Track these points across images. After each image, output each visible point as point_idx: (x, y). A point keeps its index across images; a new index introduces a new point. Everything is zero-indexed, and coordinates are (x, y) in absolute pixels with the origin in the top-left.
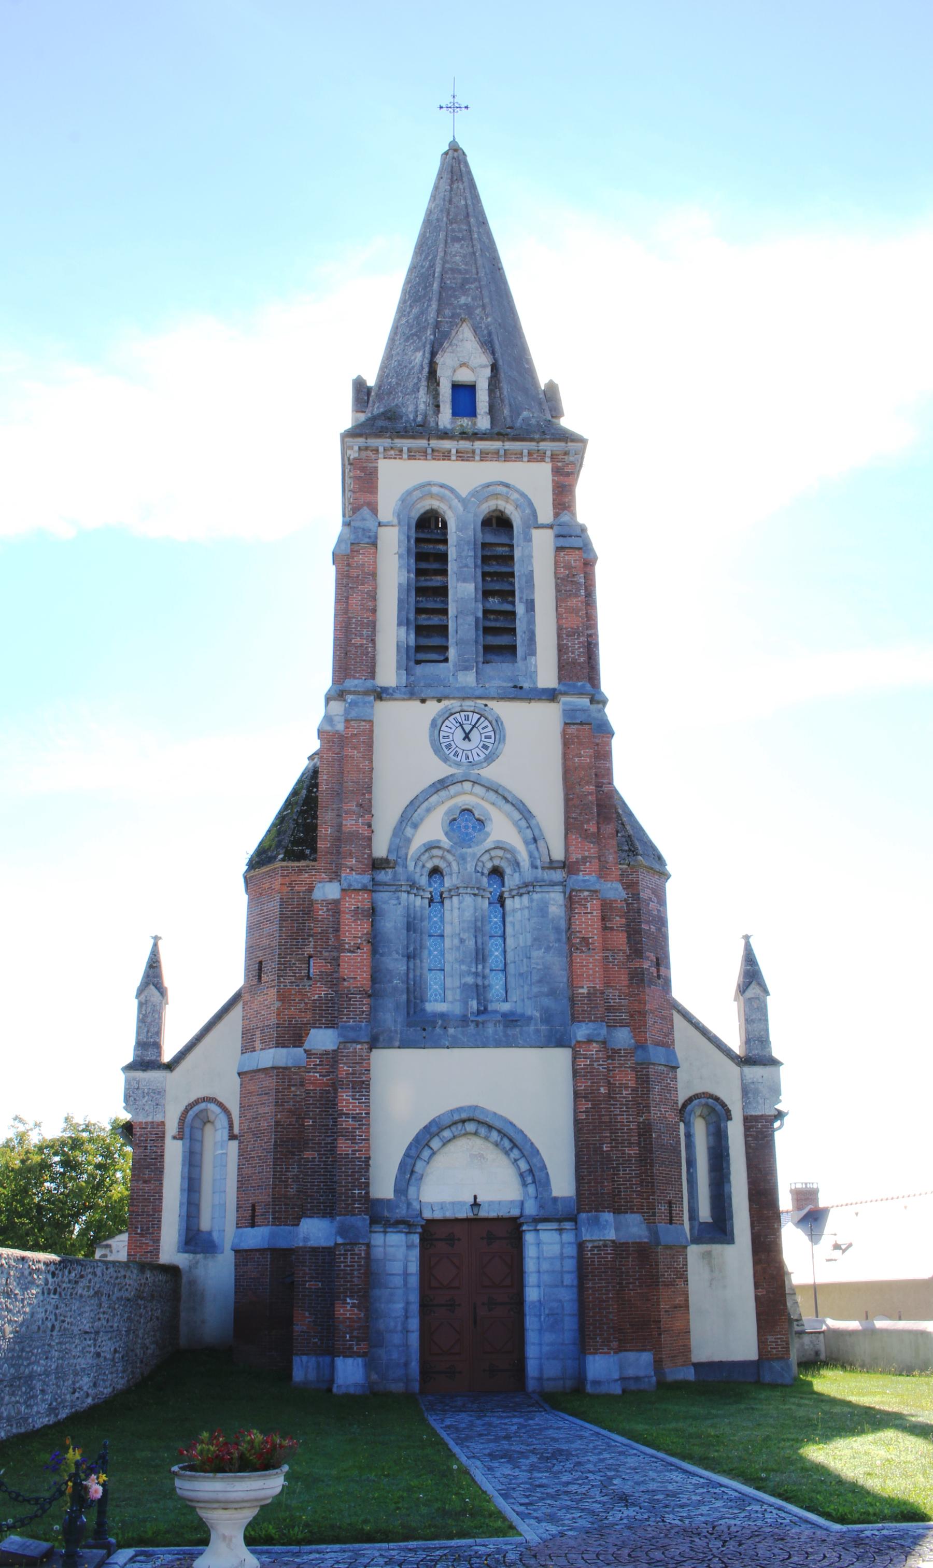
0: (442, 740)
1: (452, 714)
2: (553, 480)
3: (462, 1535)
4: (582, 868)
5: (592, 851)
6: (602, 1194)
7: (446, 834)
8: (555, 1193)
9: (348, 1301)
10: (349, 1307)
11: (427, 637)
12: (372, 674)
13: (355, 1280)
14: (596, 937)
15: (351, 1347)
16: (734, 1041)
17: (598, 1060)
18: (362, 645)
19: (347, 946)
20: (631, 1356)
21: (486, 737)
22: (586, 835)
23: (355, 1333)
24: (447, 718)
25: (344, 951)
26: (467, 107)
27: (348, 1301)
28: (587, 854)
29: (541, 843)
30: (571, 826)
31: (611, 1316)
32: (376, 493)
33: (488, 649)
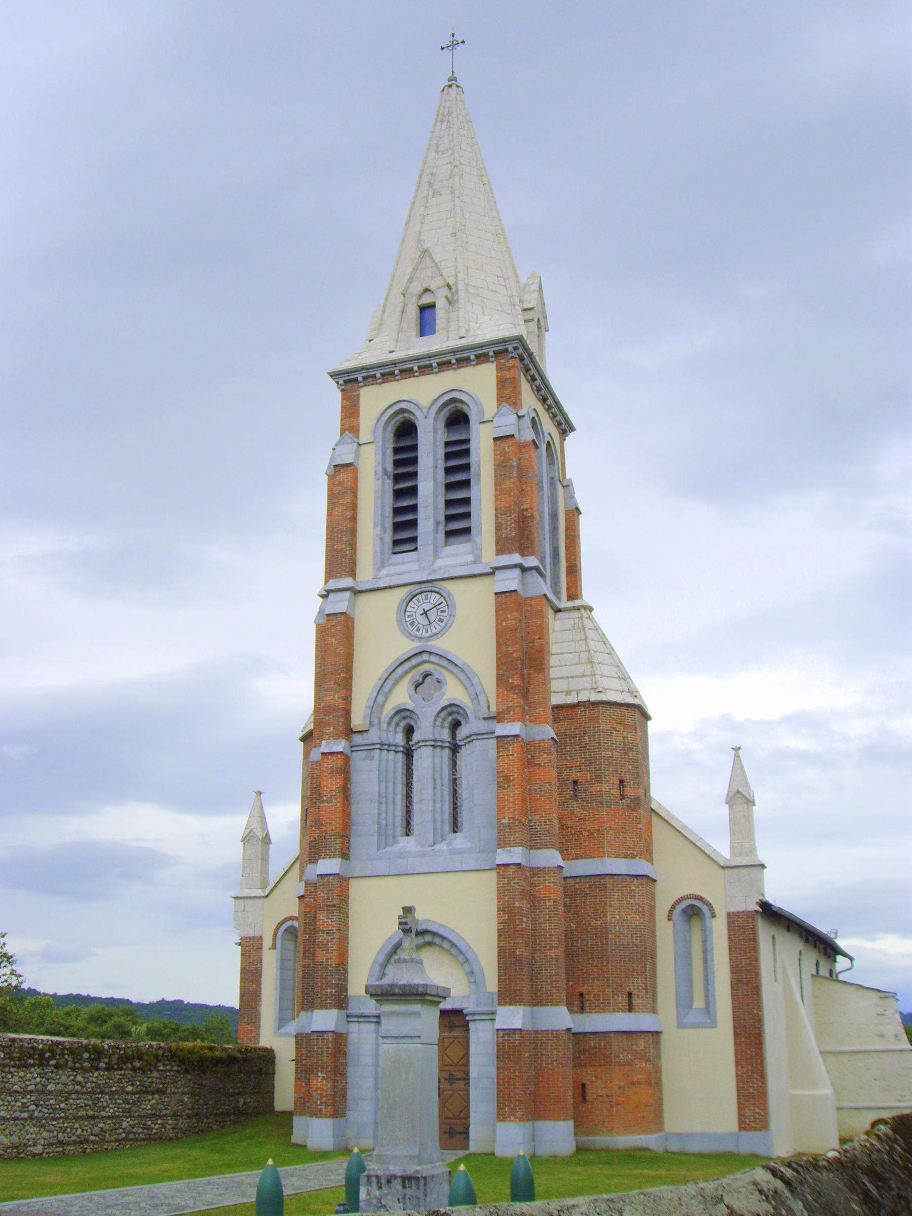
0: (407, 619)
1: (414, 596)
2: (497, 377)
3: (23, 1197)
4: (506, 716)
5: (515, 701)
6: (515, 990)
7: (410, 697)
8: (489, 990)
9: (320, 1074)
10: (320, 1079)
11: (404, 530)
12: (353, 574)
13: (325, 1059)
14: (516, 775)
15: (321, 1110)
16: (722, 848)
17: (513, 879)
18: (342, 550)
19: (325, 798)
20: (545, 1125)
21: (442, 612)
22: (512, 688)
23: (324, 1099)
24: (411, 600)
25: (323, 801)
26: (443, 49)
27: (320, 1074)
28: (511, 704)
29: (482, 698)
30: (501, 681)
31: (517, 1091)
32: (358, 417)
33: (449, 534)
